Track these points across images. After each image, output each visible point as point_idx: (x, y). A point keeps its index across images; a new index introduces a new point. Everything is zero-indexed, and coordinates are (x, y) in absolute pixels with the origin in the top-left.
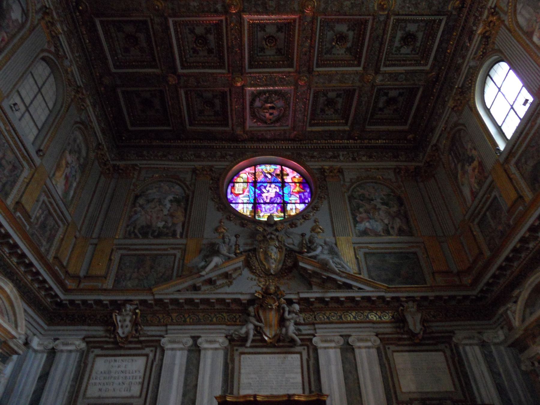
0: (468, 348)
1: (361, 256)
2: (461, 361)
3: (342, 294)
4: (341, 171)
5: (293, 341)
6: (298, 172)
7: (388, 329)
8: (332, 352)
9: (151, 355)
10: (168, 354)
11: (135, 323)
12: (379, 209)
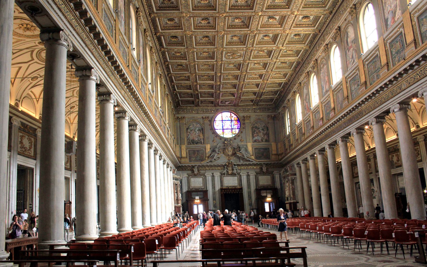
1: (254, 150)
2: (274, 177)
4: (250, 117)
5: (235, 174)
6: (236, 116)
8: (244, 176)
10: (207, 177)
11: (198, 171)
12: (261, 132)
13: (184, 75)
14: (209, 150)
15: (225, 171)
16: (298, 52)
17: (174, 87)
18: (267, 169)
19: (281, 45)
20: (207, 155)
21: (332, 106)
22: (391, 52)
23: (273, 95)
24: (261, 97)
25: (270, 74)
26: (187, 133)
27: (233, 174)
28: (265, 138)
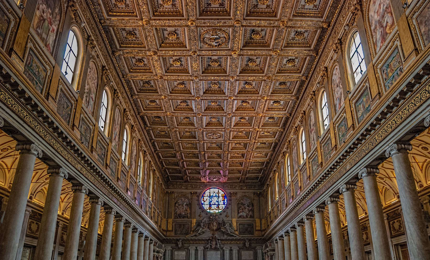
0: (259, 250)
1: (238, 225)
2: (256, 253)
3: (231, 238)
4: (236, 193)
7: (241, 245)
9: (187, 251)
10: (191, 251)
11: (182, 244)
13: (170, 152)
14: (195, 224)
15: (208, 246)
16: (274, 134)
17: (161, 163)
18: (249, 244)
19: (257, 127)
20: (192, 230)
21: (299, 185)
22: (339, 135)
23: (258, 173)
24: (246, 175)
25: (251, 154)
26: (175, 207)
27: (216, 249)
28: (250, 214)
